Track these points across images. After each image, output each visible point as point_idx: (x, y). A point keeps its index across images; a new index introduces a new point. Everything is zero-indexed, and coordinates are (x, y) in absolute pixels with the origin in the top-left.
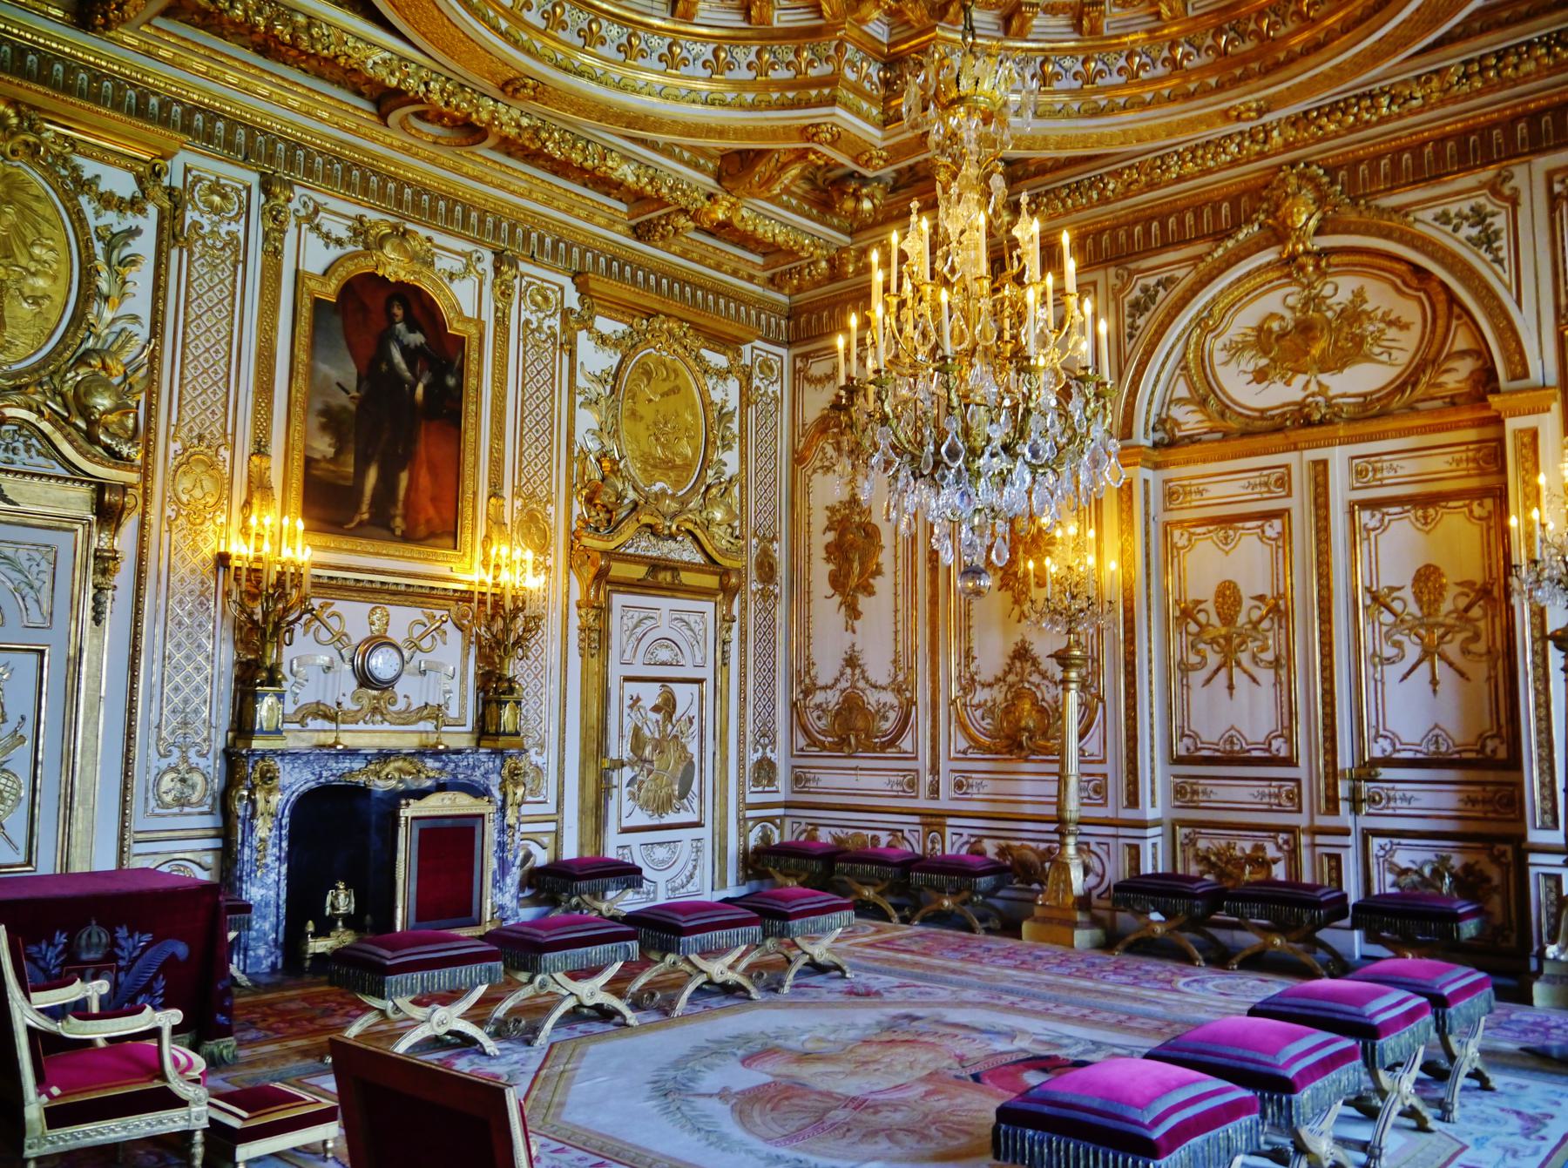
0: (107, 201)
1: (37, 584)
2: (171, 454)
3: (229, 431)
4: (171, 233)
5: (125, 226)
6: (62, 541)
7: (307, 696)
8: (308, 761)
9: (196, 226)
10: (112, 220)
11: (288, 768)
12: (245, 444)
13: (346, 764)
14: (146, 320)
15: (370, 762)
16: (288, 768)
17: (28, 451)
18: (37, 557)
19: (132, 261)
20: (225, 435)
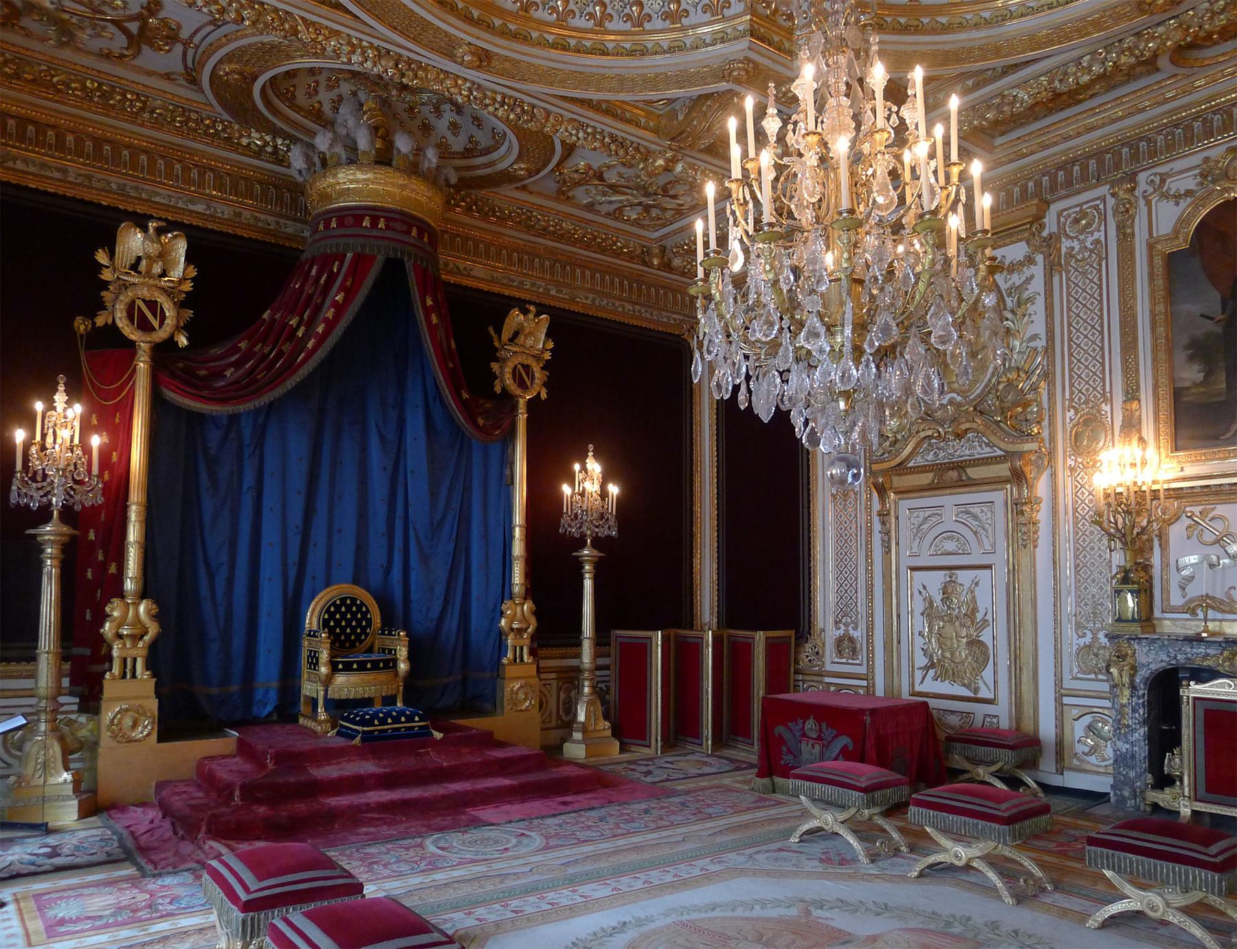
0: (1013, 268)
1: (987, 526)
2: (1068, 421)
3: (1108, 389)
4: (1051, 269)
5: (1023, 279)
6: (998, 497)
7: (1193, 591)
8: (1163, 645)
9: (1070, 255)
10: (1016, 279)
11: (1145, 650)
12: (1119, 397)
13: (1202, 650)
14: (1043, 336)
15: (1224, 649)
16: (1145, 650)
17: (980, 446)
18: (985, 509)
19: (1030, 300)
20: (1104, 395)
